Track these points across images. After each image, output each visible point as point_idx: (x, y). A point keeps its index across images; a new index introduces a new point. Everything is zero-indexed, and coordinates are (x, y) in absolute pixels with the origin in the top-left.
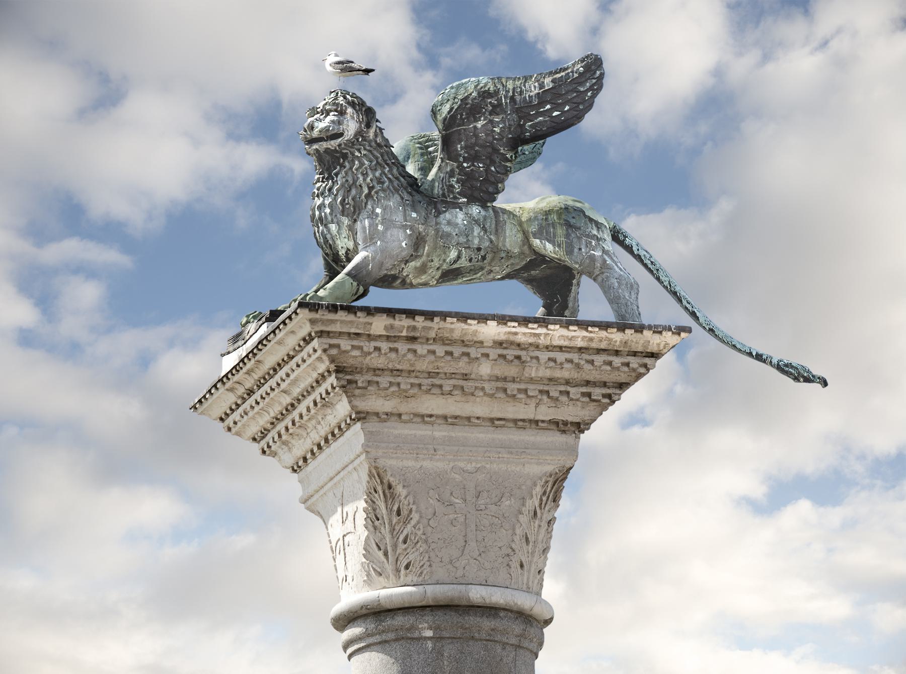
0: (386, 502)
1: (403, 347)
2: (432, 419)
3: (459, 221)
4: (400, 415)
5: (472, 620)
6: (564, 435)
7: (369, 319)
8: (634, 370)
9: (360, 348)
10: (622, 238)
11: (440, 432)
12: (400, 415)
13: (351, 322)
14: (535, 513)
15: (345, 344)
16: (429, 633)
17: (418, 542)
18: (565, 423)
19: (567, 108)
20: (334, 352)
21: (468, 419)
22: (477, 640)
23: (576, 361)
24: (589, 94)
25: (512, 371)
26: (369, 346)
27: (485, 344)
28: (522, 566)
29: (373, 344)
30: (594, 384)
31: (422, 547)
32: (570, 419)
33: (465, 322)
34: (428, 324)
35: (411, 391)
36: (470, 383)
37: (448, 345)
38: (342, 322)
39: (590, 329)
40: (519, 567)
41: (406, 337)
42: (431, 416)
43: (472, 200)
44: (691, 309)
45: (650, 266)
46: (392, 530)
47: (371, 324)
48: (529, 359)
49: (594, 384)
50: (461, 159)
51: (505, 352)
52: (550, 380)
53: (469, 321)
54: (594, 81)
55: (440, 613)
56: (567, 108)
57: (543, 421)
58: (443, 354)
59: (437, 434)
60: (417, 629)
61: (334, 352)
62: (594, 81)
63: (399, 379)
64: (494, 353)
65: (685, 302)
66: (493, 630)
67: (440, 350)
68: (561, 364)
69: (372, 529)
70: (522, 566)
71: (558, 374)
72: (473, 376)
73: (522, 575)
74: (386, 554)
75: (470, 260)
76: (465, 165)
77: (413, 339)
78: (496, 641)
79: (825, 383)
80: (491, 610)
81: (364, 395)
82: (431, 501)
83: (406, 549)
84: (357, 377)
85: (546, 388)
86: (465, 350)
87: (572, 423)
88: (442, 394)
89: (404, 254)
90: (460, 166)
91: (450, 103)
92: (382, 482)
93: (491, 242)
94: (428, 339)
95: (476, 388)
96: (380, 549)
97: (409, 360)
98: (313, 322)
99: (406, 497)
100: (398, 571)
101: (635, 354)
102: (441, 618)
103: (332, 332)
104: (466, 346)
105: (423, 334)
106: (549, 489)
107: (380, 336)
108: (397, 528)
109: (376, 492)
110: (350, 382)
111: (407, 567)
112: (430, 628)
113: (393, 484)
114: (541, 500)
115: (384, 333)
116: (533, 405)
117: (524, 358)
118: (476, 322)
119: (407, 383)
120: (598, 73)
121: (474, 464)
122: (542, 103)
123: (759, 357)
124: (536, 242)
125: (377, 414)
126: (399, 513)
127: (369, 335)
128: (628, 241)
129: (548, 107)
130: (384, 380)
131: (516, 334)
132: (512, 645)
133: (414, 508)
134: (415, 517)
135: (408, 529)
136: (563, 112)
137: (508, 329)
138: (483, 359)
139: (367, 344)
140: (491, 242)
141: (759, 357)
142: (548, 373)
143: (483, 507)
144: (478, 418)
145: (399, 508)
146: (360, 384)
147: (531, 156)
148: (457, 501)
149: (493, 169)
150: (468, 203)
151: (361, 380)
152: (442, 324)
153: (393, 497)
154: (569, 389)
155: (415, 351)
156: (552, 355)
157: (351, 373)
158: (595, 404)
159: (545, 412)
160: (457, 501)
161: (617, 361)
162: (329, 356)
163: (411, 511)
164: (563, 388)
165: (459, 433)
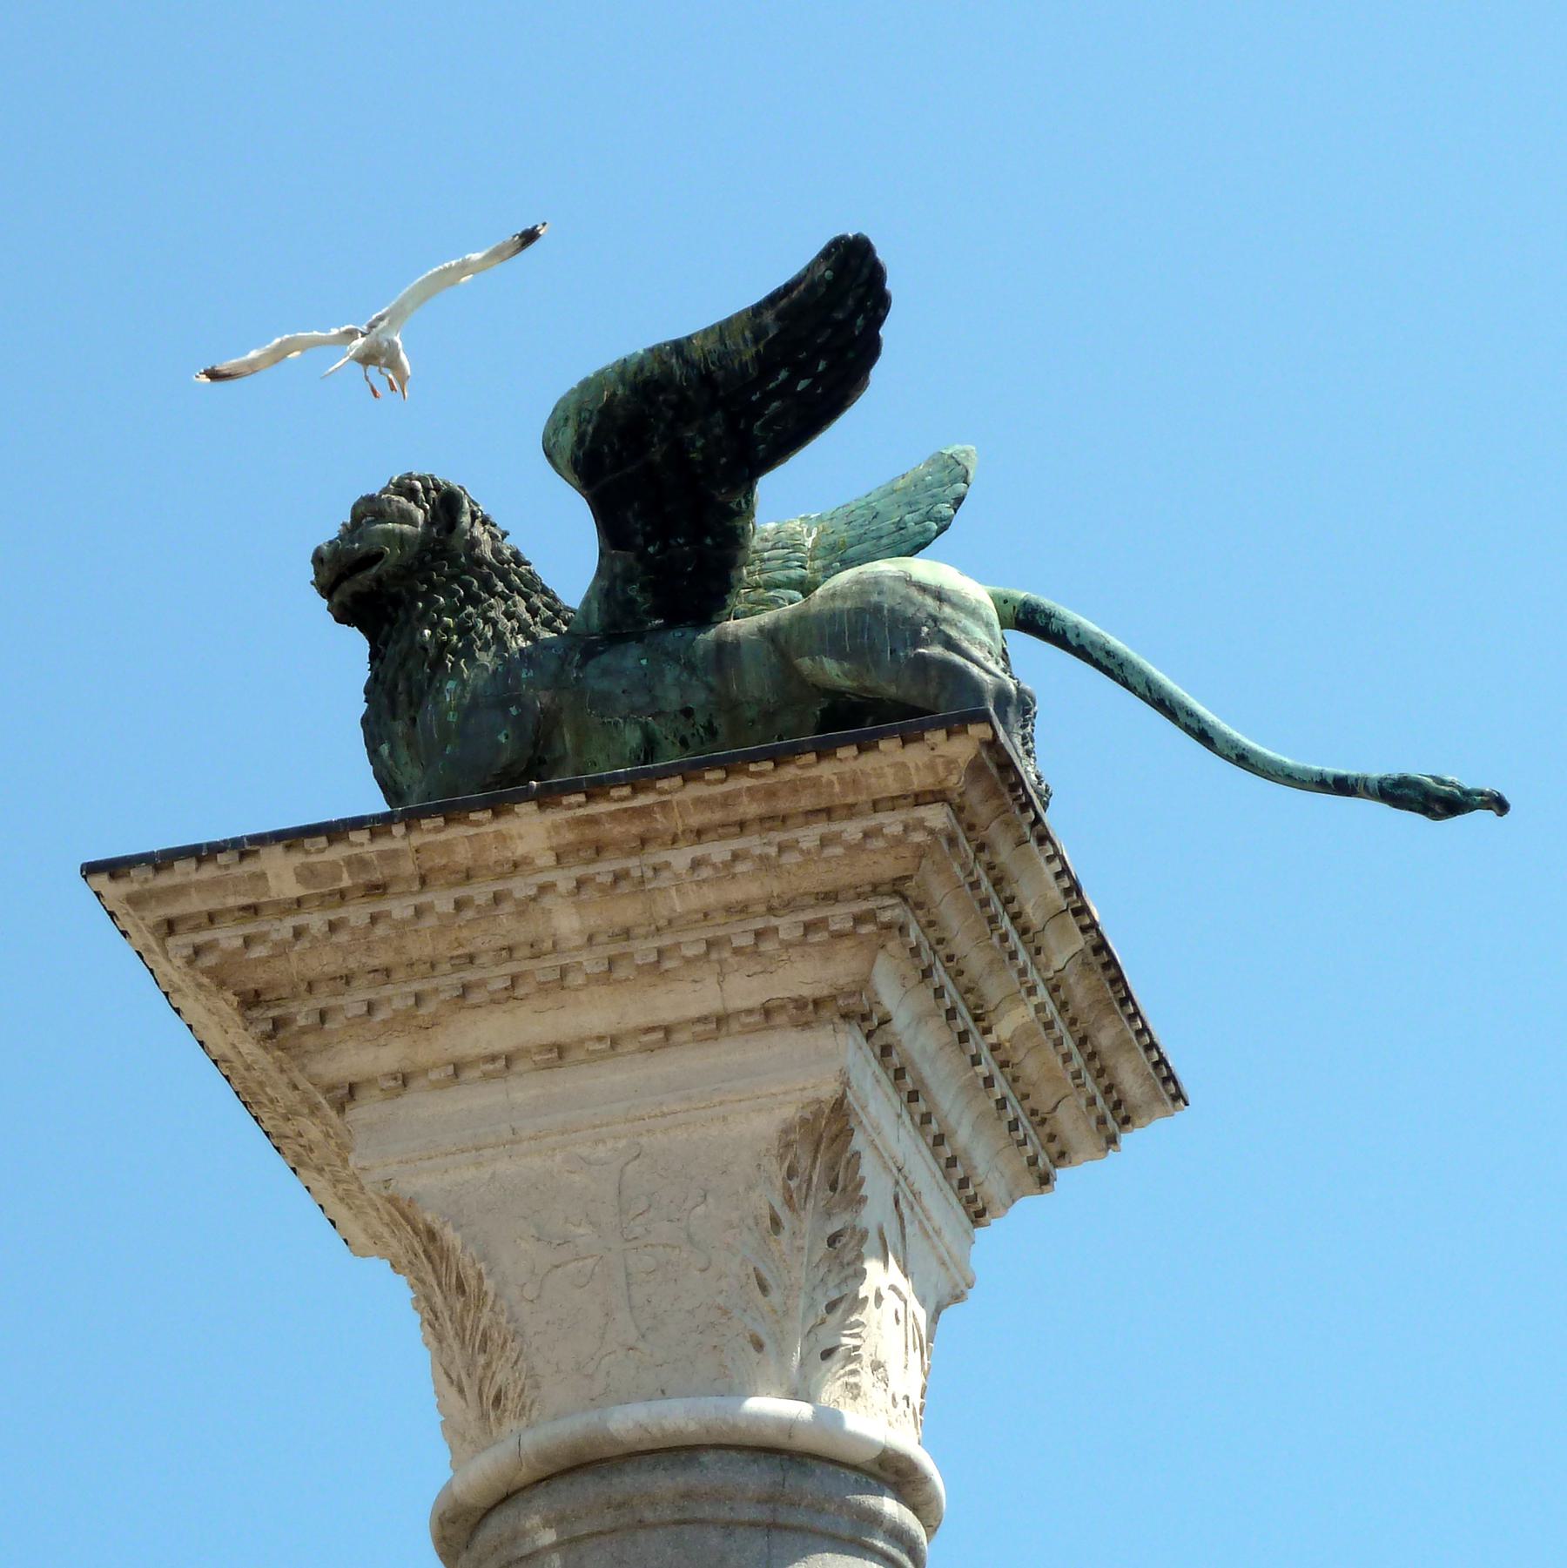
0: (435, 1270)
1: (356, 913)
5: (626, 1483)
6: (808, 1034)
7: (249, 866)
8: (898, 841)
9: (262, 938)
10: (1041, 621)
11: (524, 1090)
12: (426, 1071)
13: (216, 883)
14: (776, 1223)
15: (228, 937)
16: (548, 1537)
17: (505, 1342)
18: (800, 1003)
19: (822, 366)
20: (209, 960)
22: (653, 1526)
23: (758, 852)
24: (860, 321)
25: (627, 911)
27: (540, 862)
29: (290, 922)
30: (830, 897)
31: (512, 1350)
32: (807, 992)
33: (465, 821)
34: (384, 844)
35: (422, 1011)
36: (549, 962)
37: (457, 884)
38: (200, 886)
39: (753, 768)
41: (355, 886)
42: (493, 1058)
44: (1195, 725)
45: (1105, 662)
46: (460, 1334)
47: (262, 876)
48: (650, 873)
49: (830, 897)
50: (640, 540)
51: (591, 870)
52: (729, 909)
53: (473, 816)
54: (861, 290)
55: (561, 1485)
56: (822, 366)
57: (750, 1012)
58: (450, 908)
59: (519, 1096)
60: (525, 1534)
62: (861, 290)
63: (388, 990)
64: (564, 880)
65: (1182, 716)
66: (687, 1496)
67: (442, 901)
69: (435, 1344)
71: (736, 893)
74: (461, 1391)
75: (684, 743)
76: (651, 549)
77: (377, 889)
78: (702, 1522)
79: (1499, 805)
80: (678, 1452)
81: (328, 1046)
82: (523, 1245)
83: (488, 1365)
84: (293, 1007)
85: (720, 932)
86: (499, 886)
87: (817, 1003)
88: (493, 1002)
89: (505, 758)
90: (642, 556)
91: (571, 422)
92: (416, 1232)
93: (711, 689)
97: (385, 940)
98: (134, 901)
99: (464, 1248)
100: (484, 1416)
101: (894, 802)
102: (570, 1495)
103: (190, 917)
104: (501, 877)
105: (387, 871)
106: (805, 1162)
107: (299, 902)
108: (468, 1324)
110: (278, 1024)
111: (497, 1400)
112: (547, 1524)
113: (437, 1226)
114: (787, 1189)
115: (298, 891)
116: (711, 981)
117: (636, 873)
118: (488, 814)
119: (405, 996)
120: (866, 271)
121: (610, 1144)
123: (1342, 786)
124: (805, 664)
125: (371, 1081)
126: (461, 1287)
127: (276, 903)
128: (1054, 626)
129: (783, 374)
130: (353, 1002)
131: (592, 820)
132: (753, 1524)
133: (482, 1266)
134: (489, 1284)
135: (486, 1318)
136: (818, 379)
137: (570, 814)
139: (277, 924)
140: (711, 689)
141: (1342, 786)
142: (710, 896)
143: (639, 1231)
144: (600, 1039)
145: (458, 1277)
146: (301, 1021)
147: (917, 528)
148: (581, 1231)
149: (709, 541)
150: (670, 624)
151: (303, 1015)
152: (416, 839)
153: (445, 1254)
154: (774, 921)
155: (388, 914)
156: (699, 851)
158: (848, 943)
159: (745, 990)
160: (581, 1231)
161: (852, 830)
162: (207, 972)
163: (480, 1277)
164: (759, 924)
165: (568, 1081)
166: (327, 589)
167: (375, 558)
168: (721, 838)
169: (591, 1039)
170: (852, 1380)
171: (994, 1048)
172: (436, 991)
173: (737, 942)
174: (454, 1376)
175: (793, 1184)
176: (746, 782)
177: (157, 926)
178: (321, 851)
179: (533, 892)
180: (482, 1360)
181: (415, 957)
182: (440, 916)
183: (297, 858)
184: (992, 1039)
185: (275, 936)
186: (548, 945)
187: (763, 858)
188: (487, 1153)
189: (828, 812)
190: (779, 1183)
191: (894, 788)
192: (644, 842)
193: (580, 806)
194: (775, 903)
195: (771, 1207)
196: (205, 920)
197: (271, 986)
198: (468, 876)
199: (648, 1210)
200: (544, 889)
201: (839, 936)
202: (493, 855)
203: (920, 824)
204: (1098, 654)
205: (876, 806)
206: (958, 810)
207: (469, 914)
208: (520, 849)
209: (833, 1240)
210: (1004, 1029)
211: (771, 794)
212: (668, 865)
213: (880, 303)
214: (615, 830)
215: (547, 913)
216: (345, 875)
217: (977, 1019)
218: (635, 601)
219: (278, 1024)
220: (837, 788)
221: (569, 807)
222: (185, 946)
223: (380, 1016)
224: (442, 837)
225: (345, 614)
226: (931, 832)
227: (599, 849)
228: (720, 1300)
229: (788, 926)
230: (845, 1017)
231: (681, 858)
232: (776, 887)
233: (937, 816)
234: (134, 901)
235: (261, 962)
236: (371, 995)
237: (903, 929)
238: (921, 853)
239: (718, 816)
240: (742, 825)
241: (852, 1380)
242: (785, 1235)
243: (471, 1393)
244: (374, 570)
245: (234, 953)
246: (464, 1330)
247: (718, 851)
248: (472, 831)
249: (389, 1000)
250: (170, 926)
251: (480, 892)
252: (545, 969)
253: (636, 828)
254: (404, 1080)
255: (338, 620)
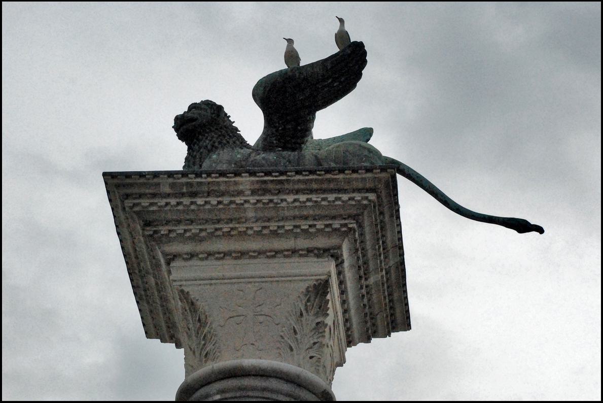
1: (186, 201)
2: (222, 255)
3: (271, 158)
4: (197, 255)
6: (320, 260)
12: (197, 255)
14: (301, 315)
15: (145, 202)
18: (319, 249)
19: (343, 79)
20: (137, 209)
21: (248, 253)
23: (315, 199)
26: (162, 202)
28: (291, 349)
34: (199, 180)
40: (289, 351)
41: (187, 193)
42: (219, 253)
43: (285, 148)
44: (444, 199)
45: (416, 179)
48: (279, 202)
49: (334, 218)
51: (261, 198)
57: (302, 250)
61: (137, 209)
65: (439, 196)
67: (214, 201)
68: (304, 202)
70: (291, 349)
72: (244, 220)
73: (293, 355)
74: (194, 352)
77: (194, 195)
83: (204, 345)
84: (161, 228)
85: (298, 224)
94: (203, 192)
95: (247, 228)
96: (191, 349)
97: (193, 210)
100: (201, 361)
101: (359, 190)
104: (233, 196)
106: (312, 299)
109: (186, 311)
113: (194, 301)
114: (306, 305)
122: (324, 79)
126: (199, 320)
127: (160, 194)
130: (180, 229)
131: (265, 182)
136: (341, 83)
137: (257, 179)
138: (246, 205)
139: (160, 201)
144: (254, 252)
152: (209, 180)
154: (315, 223)
156: (296, 197)
157: (155, 226)
159: (303, 243)
161: (345, 197)
164: (311, 223)
166: (177, 128)
167: (196, 120)
168: (304, 194)
169: (251, 251)
170: (317, 368)
171: (367, 286)
172: (206, 229)
173: (303, 227)
174: (192, 348)
175: (308, 304)
176: (315, 177)
177: (123, 195)
178: (179, 179)
179: (242, 202)
180: (203, 342)
181: (201, 217)
182: (212, 205)
183: (171, 180)
184: (368, 282)
185: (159, 204)
186: (244, 220)
187: (316, 202)
188: (213, 282)
189: (339, 191)
190: (304, 302)
191: (360, 185)
192: (279, 192)
193: (262, 176)
194: (317, 218)
195: (301, 309)
196: (138, 196)
197: (154, 221)
198: (223, 194)
199: (262, 304)
200: (246, 201)
201: (336, 230)
202: (232, 188)
203: (367, 198)
204: (414, 177)
205: (354, 191)
206: (378, 197)
207: (221, 206)
208: (241, 187)
209: (318, 324)
210: (372, 280)
211: (322, 181)
212: (285, 200)
213: (364, 63)
214: (270, 186)
215: (245, 210)
216: (185, 188)
217: (365, 274)
218: (273, 143)
219: (156, 232)
220: (343, 183)
221: (258, 177)
222: (131, 203)
223: (188, 234)
224: (217, 180)
225: (182, 136)
226: (370, 201)
227: (266, 191)
228: (282, 334)
229: (320, 225)
230: (332, 256)
231: (290, 198)
232: (318, 212)
233: (372, 196)
234: (118, 186)
235: (153, 212)
236: (186, 228)
237: (355, 231)
238: (366, 206)
239: (302, 186)
240: (312, 191)
241: (317, 368)
242: (303, 319)
243: (197, 354)
244: (194, 123)
245: (147, 207)
246: (198, 333)
247: (303, 198)
248: (227, 180)
249: (191, 230)
250: (127, 196)
251: (226, 200)
252: (242, 228)
253: (278, 187)
254: (192, 256)
255: (179, 139)
